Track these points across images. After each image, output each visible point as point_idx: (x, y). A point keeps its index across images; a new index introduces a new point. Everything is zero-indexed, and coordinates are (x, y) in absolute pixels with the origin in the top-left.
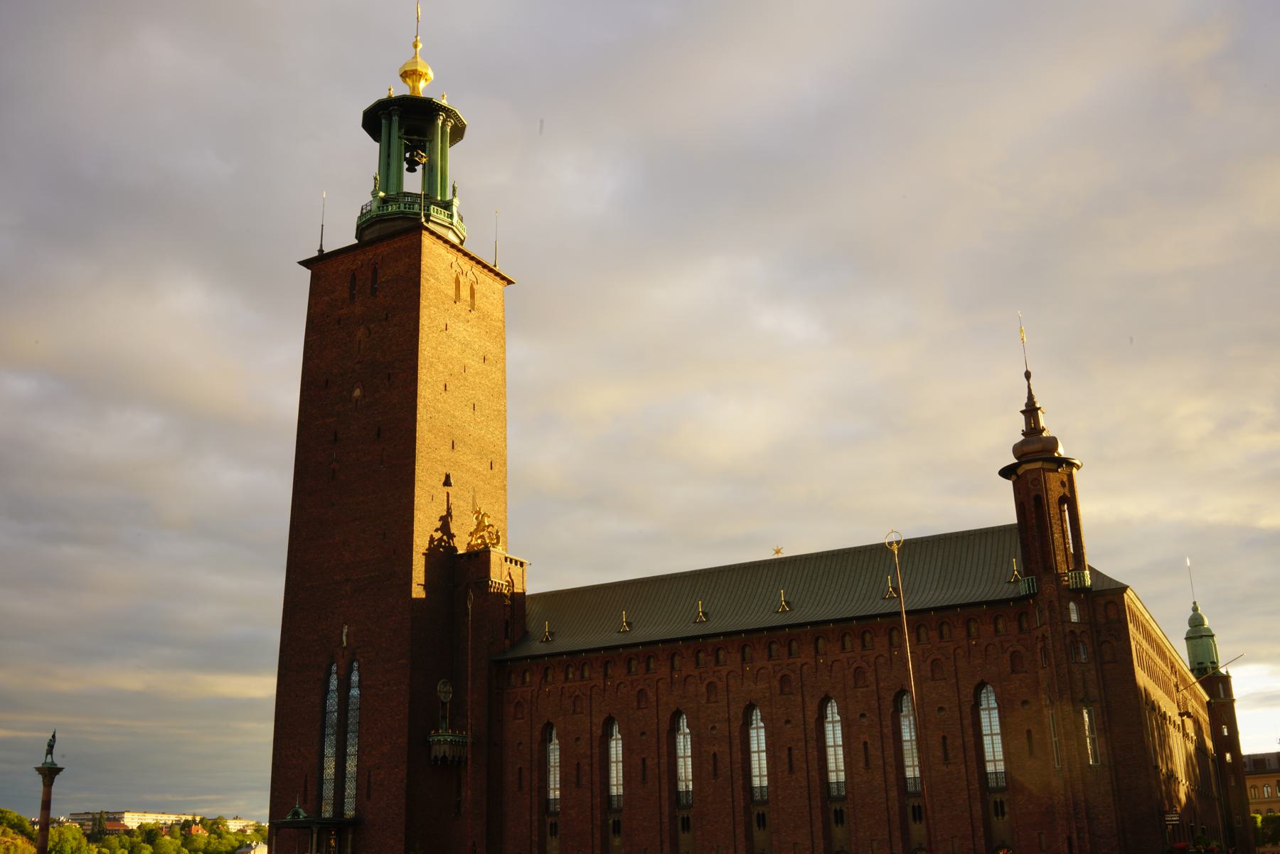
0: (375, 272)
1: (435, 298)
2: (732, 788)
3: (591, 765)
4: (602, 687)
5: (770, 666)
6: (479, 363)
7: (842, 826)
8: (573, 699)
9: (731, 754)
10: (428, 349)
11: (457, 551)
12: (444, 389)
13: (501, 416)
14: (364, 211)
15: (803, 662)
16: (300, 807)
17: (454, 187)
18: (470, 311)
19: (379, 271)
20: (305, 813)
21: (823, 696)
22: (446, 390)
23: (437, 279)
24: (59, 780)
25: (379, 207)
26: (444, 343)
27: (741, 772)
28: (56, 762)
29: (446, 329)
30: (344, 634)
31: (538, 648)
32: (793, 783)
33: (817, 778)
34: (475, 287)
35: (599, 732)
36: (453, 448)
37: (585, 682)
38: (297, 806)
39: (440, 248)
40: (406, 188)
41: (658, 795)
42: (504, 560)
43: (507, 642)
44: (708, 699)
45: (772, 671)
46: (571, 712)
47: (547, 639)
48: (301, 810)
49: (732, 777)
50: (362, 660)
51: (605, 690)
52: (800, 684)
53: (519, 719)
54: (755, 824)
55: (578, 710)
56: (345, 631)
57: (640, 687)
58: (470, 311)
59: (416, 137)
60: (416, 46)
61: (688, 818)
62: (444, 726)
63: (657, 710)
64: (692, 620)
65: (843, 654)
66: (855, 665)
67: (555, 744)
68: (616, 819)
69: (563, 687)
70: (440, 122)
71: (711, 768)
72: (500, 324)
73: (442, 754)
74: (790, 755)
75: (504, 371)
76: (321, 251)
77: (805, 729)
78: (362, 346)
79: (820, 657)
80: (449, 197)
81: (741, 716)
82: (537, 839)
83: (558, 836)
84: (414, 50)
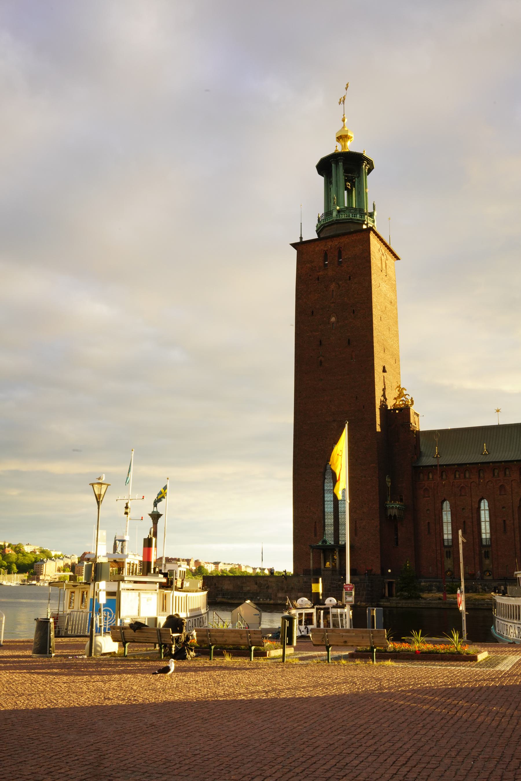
0: (340, 253)
4: (478, 483)
11: (388, 408)
13: (397, 335)
19: (343, 252)
23: (375, 258)
24: (160, 520)
25: (337, 215)
28: (158, 511)
34: (387, 262)
35: (477, 506)
37: (467, 480)
51: (479, 484)
53: (426, 497)
57: (501, 484)
59: (350, 175)
60: (344, 121)
67: (447, 511)
68: (487, 551)
70: (364, 166)
72: (394, 283)
73: (394, 514)
75: (397, 309)
76: (301, 238)
78: (335, 294)
80: (370, 210)
83: (451, 558)
84: (343, 123)
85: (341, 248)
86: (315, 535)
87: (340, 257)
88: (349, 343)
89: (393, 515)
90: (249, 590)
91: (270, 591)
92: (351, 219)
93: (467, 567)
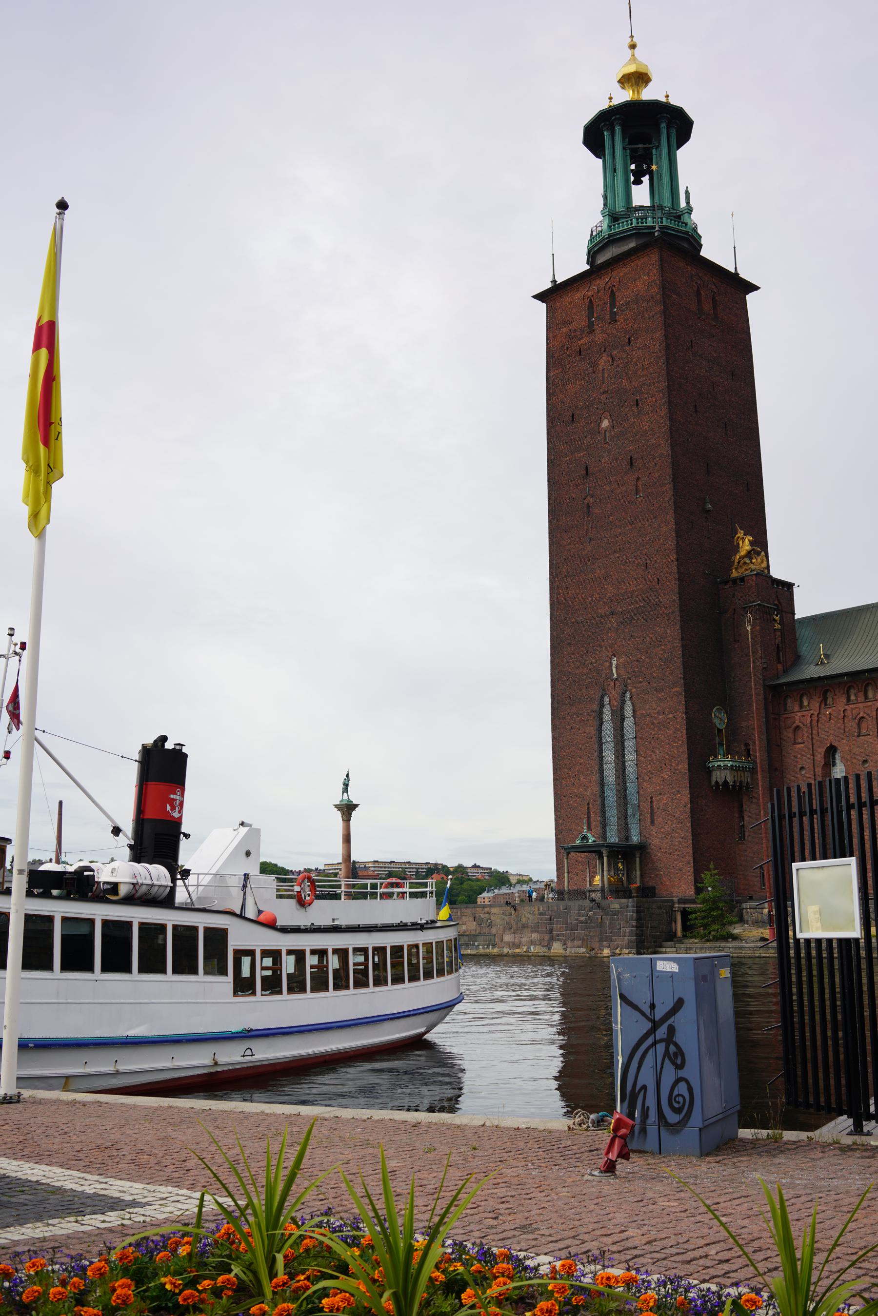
0: (613, 295)
14: (594, 233)
19: (617, 294)
22: (696, 411)
24: (354, 813)
25: (610, 227)
31: (811, 671)
37: (869, 704)
40: (636, 203)
42: (770, 583)
43: (780, 667)
48: (589, 835)
50: (634, 690)
55: (864, 732)
56: (614, 662)
59: (641, 146)
60: (633, 47)
62: (722, 752)
76: (554, 281)
78: (606, 376)
85: (614, 286)
87: (613, 304)
88: (631, 464)
89: (721, 781)
90: (465, 931)
91: (494, 931)
92: (636, 228)
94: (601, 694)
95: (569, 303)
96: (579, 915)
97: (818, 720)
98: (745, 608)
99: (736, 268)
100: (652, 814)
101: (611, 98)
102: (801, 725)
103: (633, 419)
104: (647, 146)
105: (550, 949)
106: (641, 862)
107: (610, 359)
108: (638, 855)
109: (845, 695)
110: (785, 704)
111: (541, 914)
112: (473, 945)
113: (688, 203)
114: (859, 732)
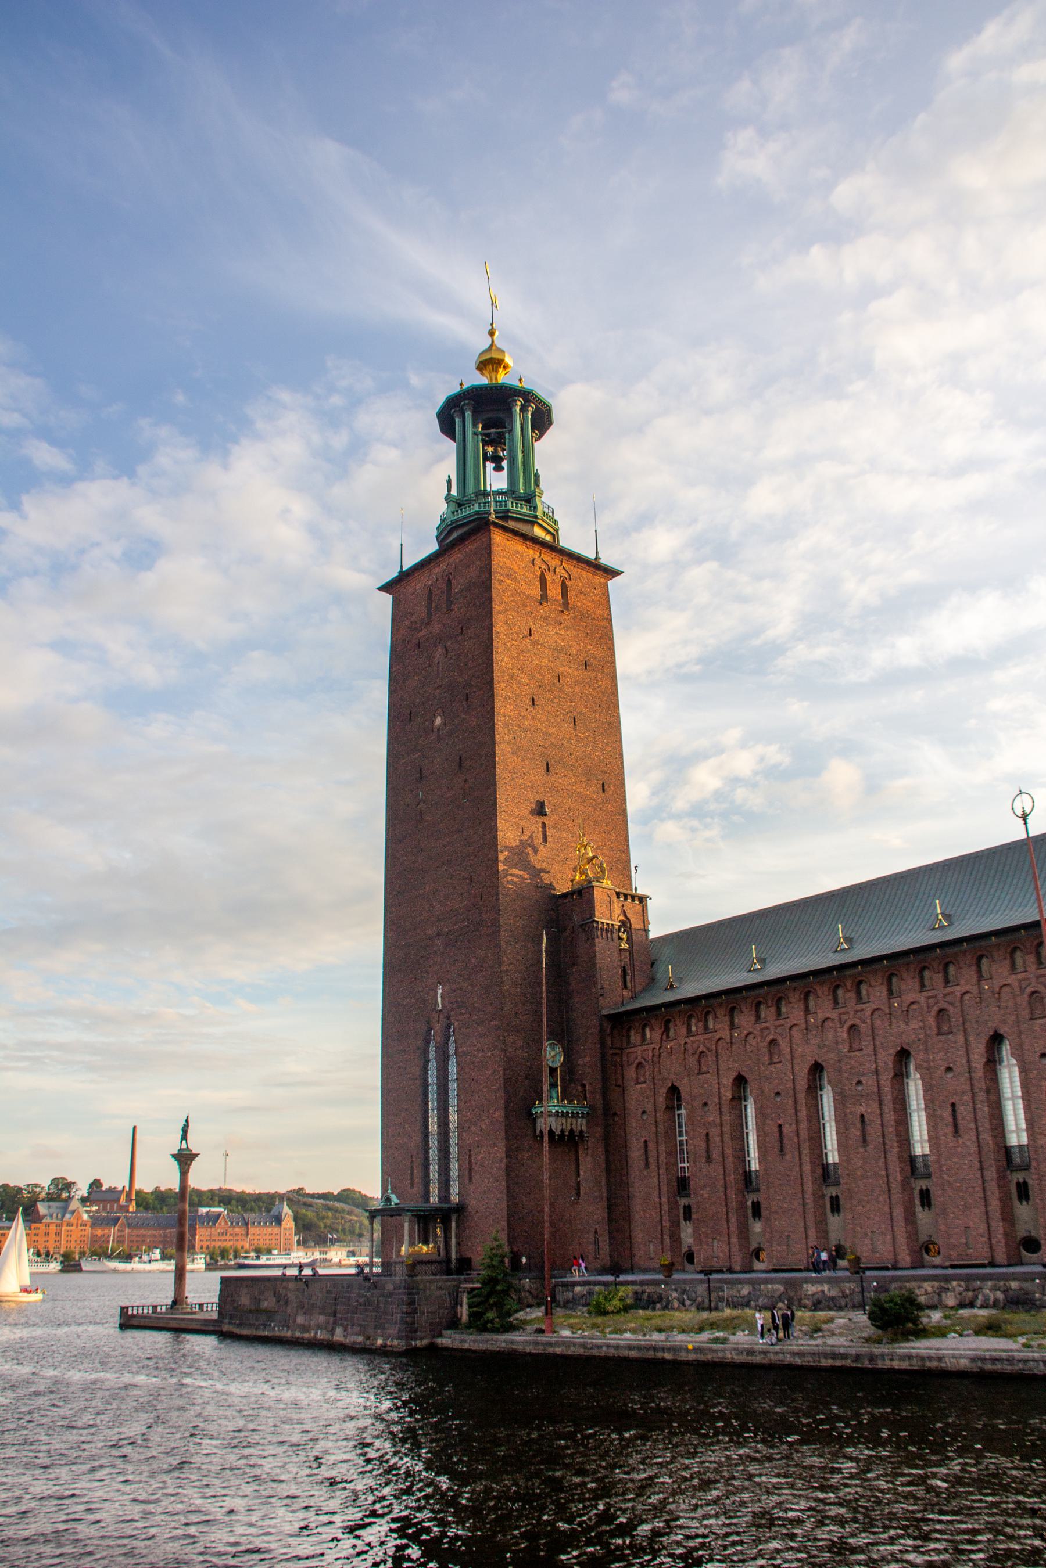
1: (513, 601)
2: (886, 1157)
3: (722, 1135)
4: (728, 1040)
5: (923, 1000)
6: (578, 669)
7: (1028, 1204)
8: (697, 1056)
9: (881, 1115)
10: (506, 659)
12: (531, 703)
15: (963, 991)
16: (392, 1193)
17: (537, 476)
18: (562, 612)
20: (398, 1198)
21: (991, 1034)
22: (533, 704)
23: (515, 580)
24: (195, 1166)
26: (529, 651)
27: (895, 1138)
29: (530, 635)
30: (439, 995)
32: (959, 1149)
33: (991, 1142)
35: (729, 1095)
36: (548, 770)
37: (710, 1035)
38: (389, 1191)
39: (517, 546)
41: (798, 1169)
43: (625, 992)
44: (851, 1047)
45: (925, 1005)
46: (696, 1072)
47: (672, 986)
49: (884, 1144)
50: (456, 1023)
52: (961, 1019)
53: (642, 1083)
54: (917, 1202)
55: (704, 1069)
56: (440, 991)
57: (771, 1037)
58: (562, 612)
59: (493, 431)
60: (492, 333)
61: (837, 1197)
62: (554, 1095)
63: (792, 1064)
64: (834, 950)
65: (1014, 976)
66: (1030, 990)
69: (686, 1043)
71: (858, 1133)
74: (954, 1111)
77: (971, 1079)
79: (983, 982)
81: (891, 1066)
82: (668, 1225)
86: (412, 1186)
91: (289, 1310)
92: (477, 513)
93: (715, 1241)
94: (426, 1028)
95: (412, 595)
96: (359, 1295)
97: (660, 1054)
98: (582, 925)
99: (597, 553)
100: (470, 1170)
101: (461, 384)
102: (643, 1062)
103: (462, 716)
104: (500, 430)
105: (333, 1335)
106: (457, 1227)
107: (444, 650)
108: (454, 1218)
109: (685, 1026)
110: (628, 1037)
111: (328, 1292)
112: (270, 1325)
113: (537, 485)
114: (700, 1070)
